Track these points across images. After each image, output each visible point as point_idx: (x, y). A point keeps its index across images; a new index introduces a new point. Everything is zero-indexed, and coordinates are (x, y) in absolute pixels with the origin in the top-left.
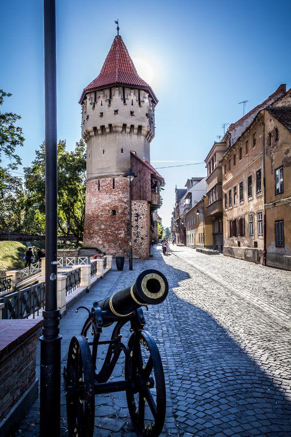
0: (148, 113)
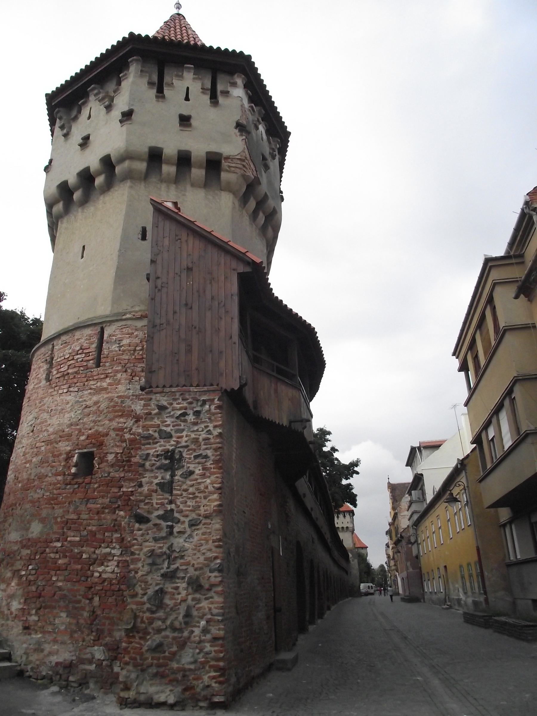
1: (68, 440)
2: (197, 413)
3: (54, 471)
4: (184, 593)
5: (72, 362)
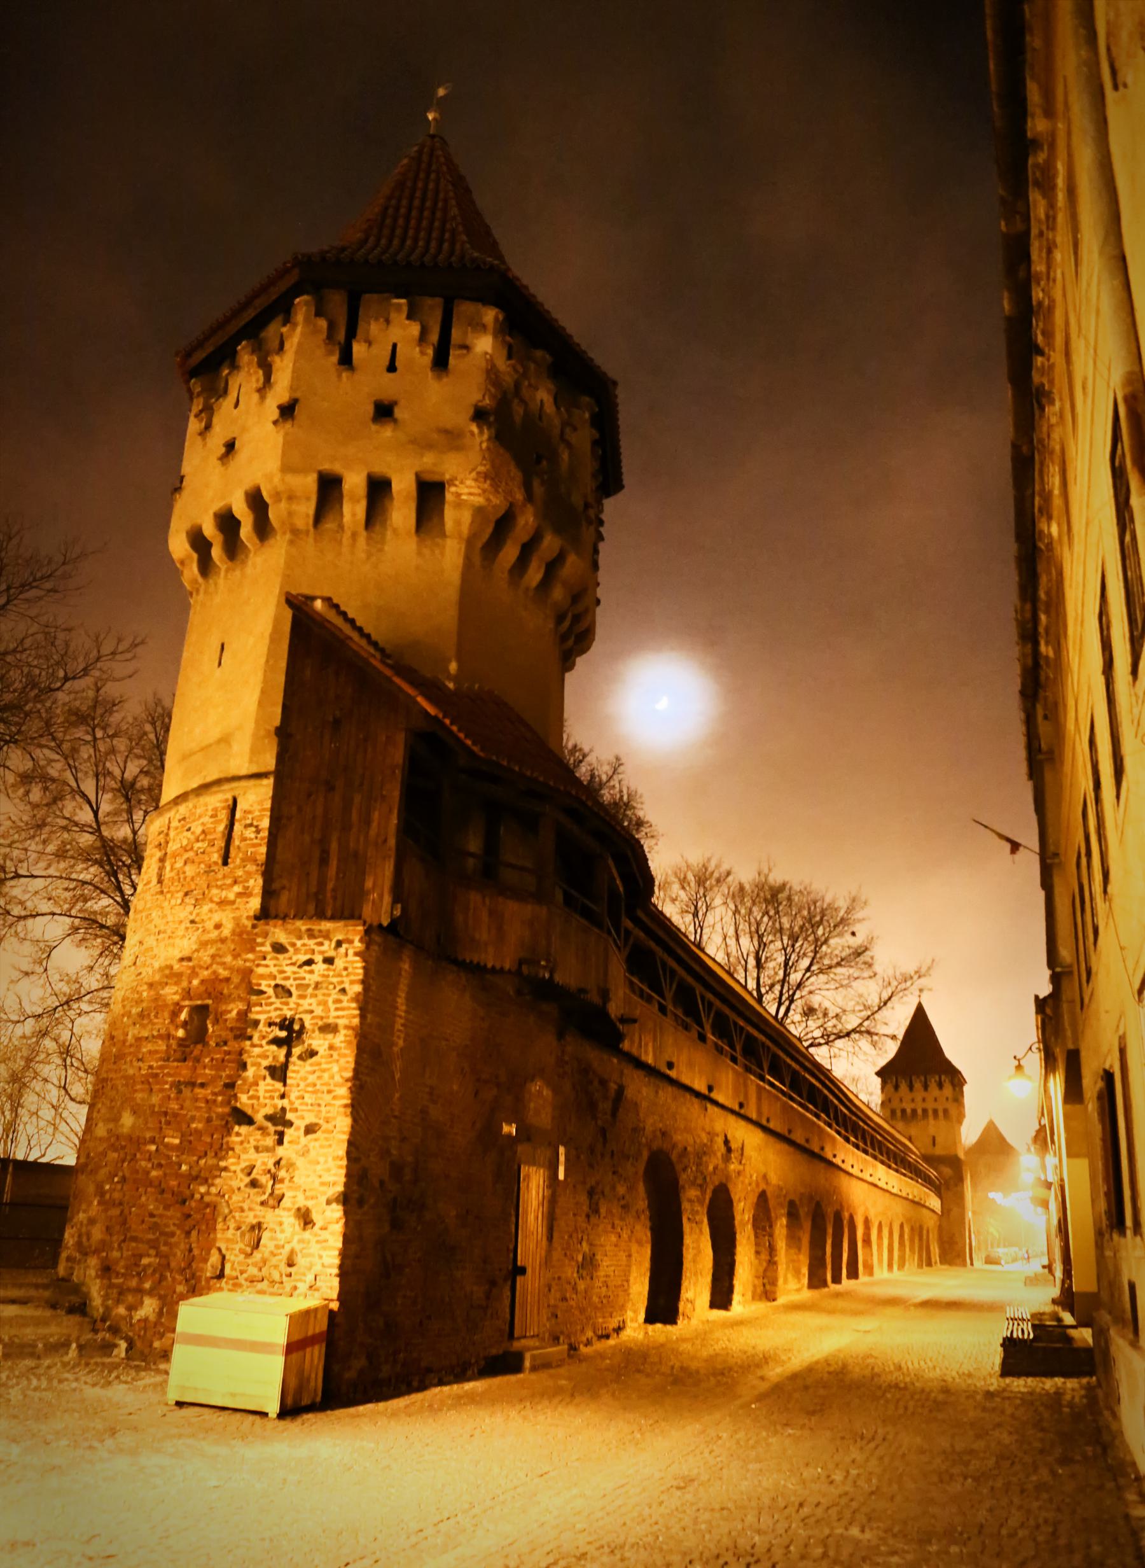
1: (176, 984)
4: (288, 1233)
5: (191, 854)
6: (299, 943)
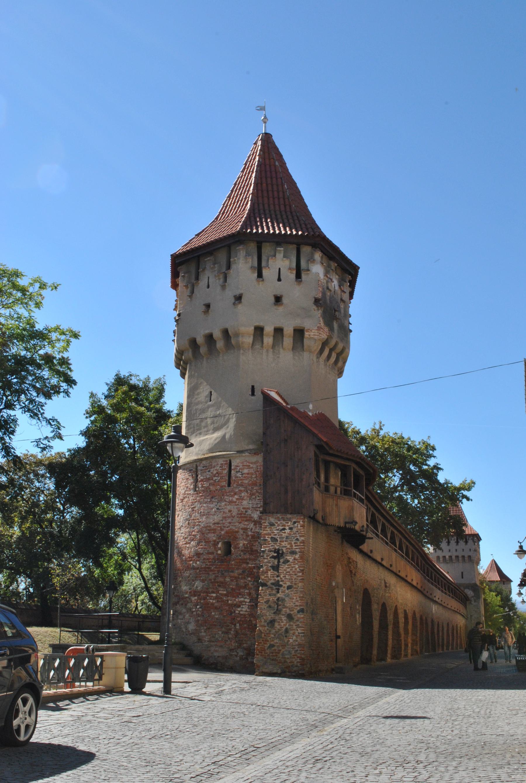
0: (320, 296)
1: (214, 533)
2: (291, 529)
3: (206, 552)
5: (211, 481)
6: (279, 522)
